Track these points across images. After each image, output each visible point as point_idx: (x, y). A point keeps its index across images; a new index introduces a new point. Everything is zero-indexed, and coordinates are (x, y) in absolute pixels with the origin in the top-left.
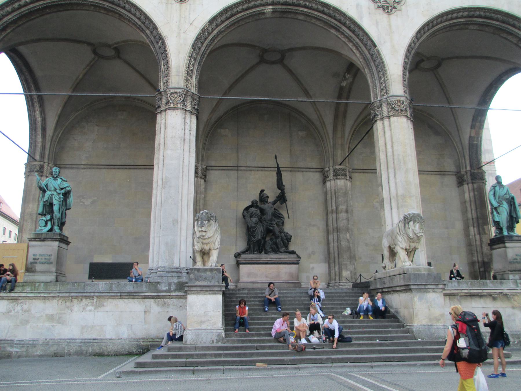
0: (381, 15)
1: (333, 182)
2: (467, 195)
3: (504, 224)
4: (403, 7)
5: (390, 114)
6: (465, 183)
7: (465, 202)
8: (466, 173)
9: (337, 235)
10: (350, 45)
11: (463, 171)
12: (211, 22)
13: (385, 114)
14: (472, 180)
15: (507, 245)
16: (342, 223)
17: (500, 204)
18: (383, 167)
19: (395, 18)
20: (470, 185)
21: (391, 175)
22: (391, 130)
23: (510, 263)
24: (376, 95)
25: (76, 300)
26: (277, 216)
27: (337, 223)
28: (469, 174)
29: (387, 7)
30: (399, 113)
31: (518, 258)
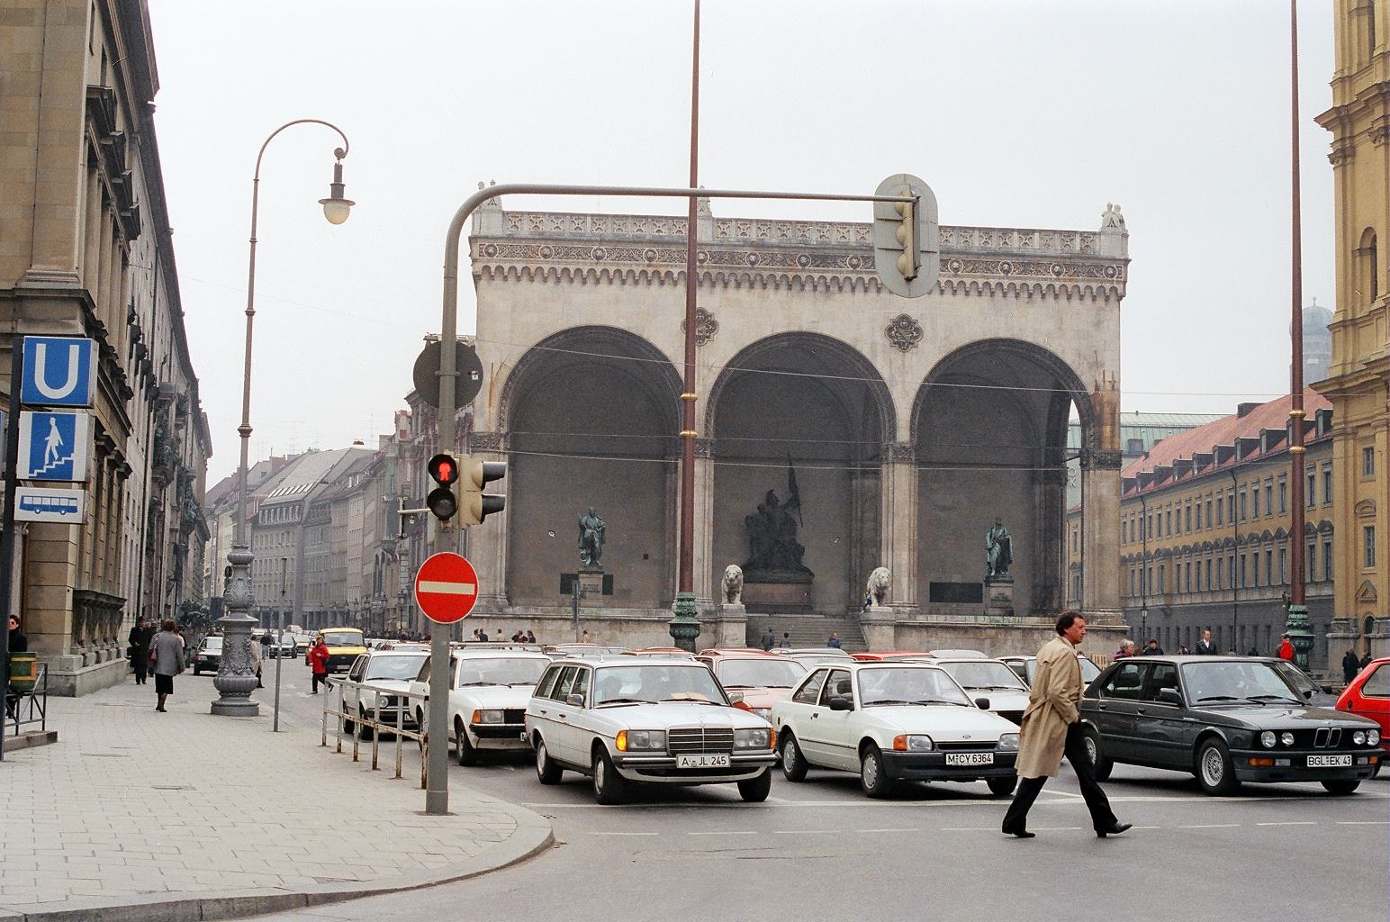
0: (896, 355)
1: (860, 480)
2: (1037, 499)
3: (993, 565)
4: (920, 343)
6: (1037, 482)
12: (728, 365)
13: (890, 459)
15: (992, 585)
17: (993, 545)
18: (884, 509)
19: (912, 357)
23: (992, 600)
26: (790, 525)
29: (904, 343)
30: (903, 461)
31: (1000, 597)
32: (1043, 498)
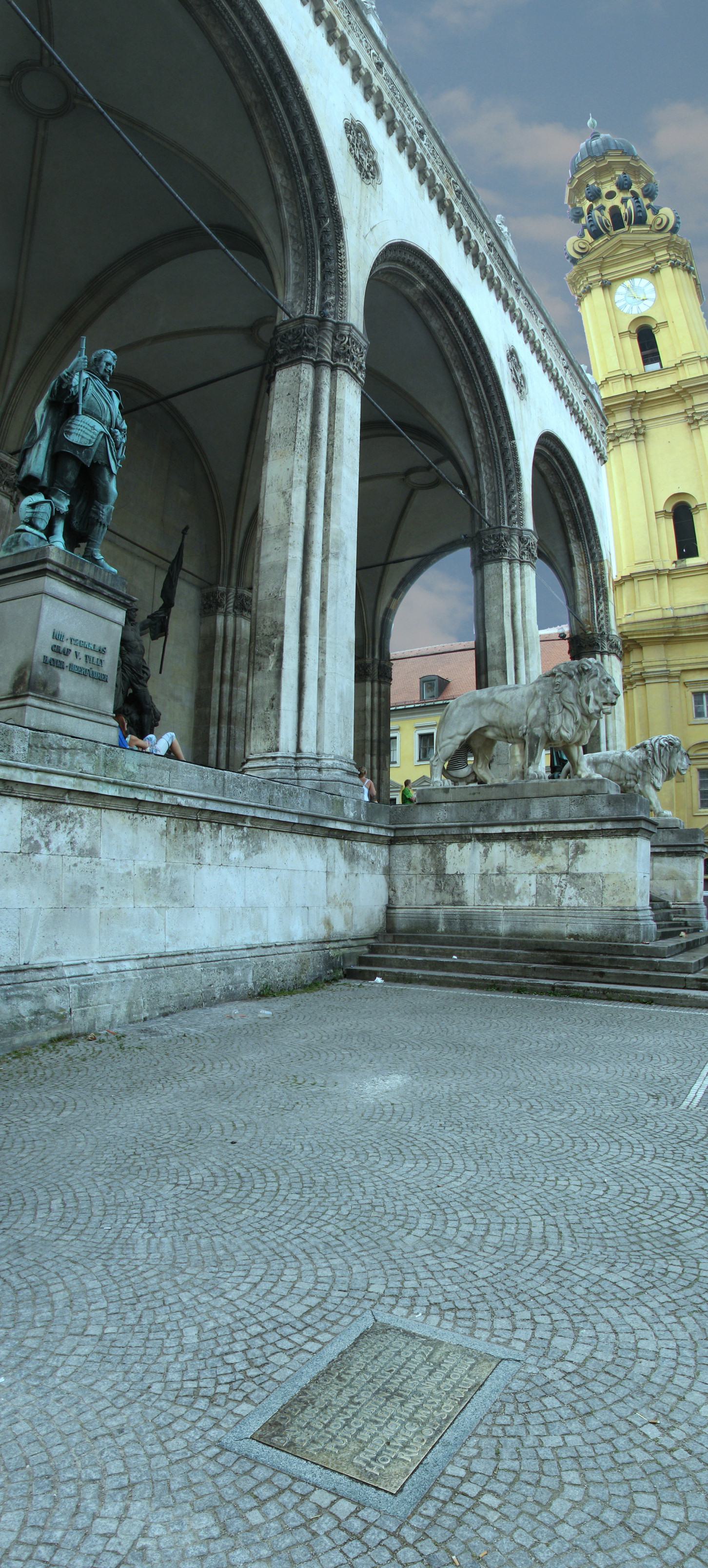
5: (525, 558)
7: (365, 710)
8: (373, 662)
9: (229, 730)
10: (472, 413)
11: (369, 660)
13: (517, 555)
14: (380, 676)
16: (240, 707)
20: (376, 684)
21: (521, 657)
22: (522, 584)
24: (498, 517)
25: (208, 825)
27: (230, 705)
28: (376, 666)
32: (376, 699)
